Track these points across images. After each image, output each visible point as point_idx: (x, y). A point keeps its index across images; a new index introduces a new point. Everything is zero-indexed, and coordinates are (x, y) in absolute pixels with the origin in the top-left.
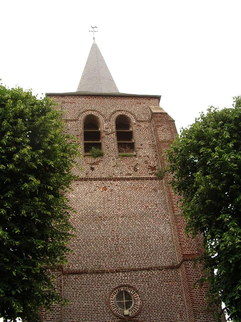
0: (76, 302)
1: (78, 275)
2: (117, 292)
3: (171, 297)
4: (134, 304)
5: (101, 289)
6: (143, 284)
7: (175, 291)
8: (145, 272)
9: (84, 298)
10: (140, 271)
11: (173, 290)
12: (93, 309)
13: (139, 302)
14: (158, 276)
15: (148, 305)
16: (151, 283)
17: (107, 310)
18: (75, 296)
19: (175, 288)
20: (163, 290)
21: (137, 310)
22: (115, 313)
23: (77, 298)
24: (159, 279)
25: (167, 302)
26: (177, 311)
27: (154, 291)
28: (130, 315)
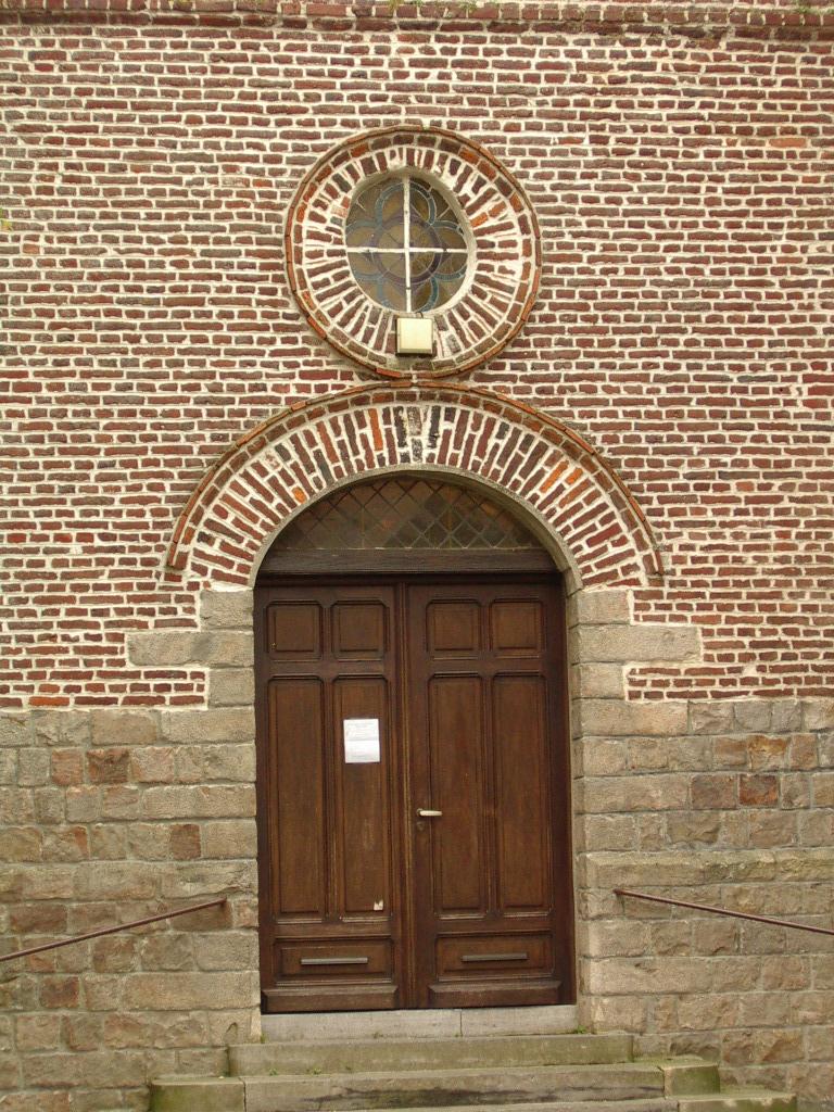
0: (42, 235)
1: (64, 31)
2: (355, 175)
3: (762, 249)
4: (478, 279)
5: (239, 147)
6: (554, 136)
7: (794, 209)
8: (580, 47)
9: (104, 204)
10: (545, 36)
11: (784, 197)
12: (167, 295)
13: (516, 266)
14: (679, 87)
15: (583, 295)
16: (623, 129)
17: (274, 304)
18: (39, 191)
19: (799, 184)
20: (702, 196)
21: (492, 322)
22: (335, 332)
23: (47, 203)
24: (683, 105)
25: (728, 283)
26: (793, 355)
27: (635, 194)
28: (439, 358)
